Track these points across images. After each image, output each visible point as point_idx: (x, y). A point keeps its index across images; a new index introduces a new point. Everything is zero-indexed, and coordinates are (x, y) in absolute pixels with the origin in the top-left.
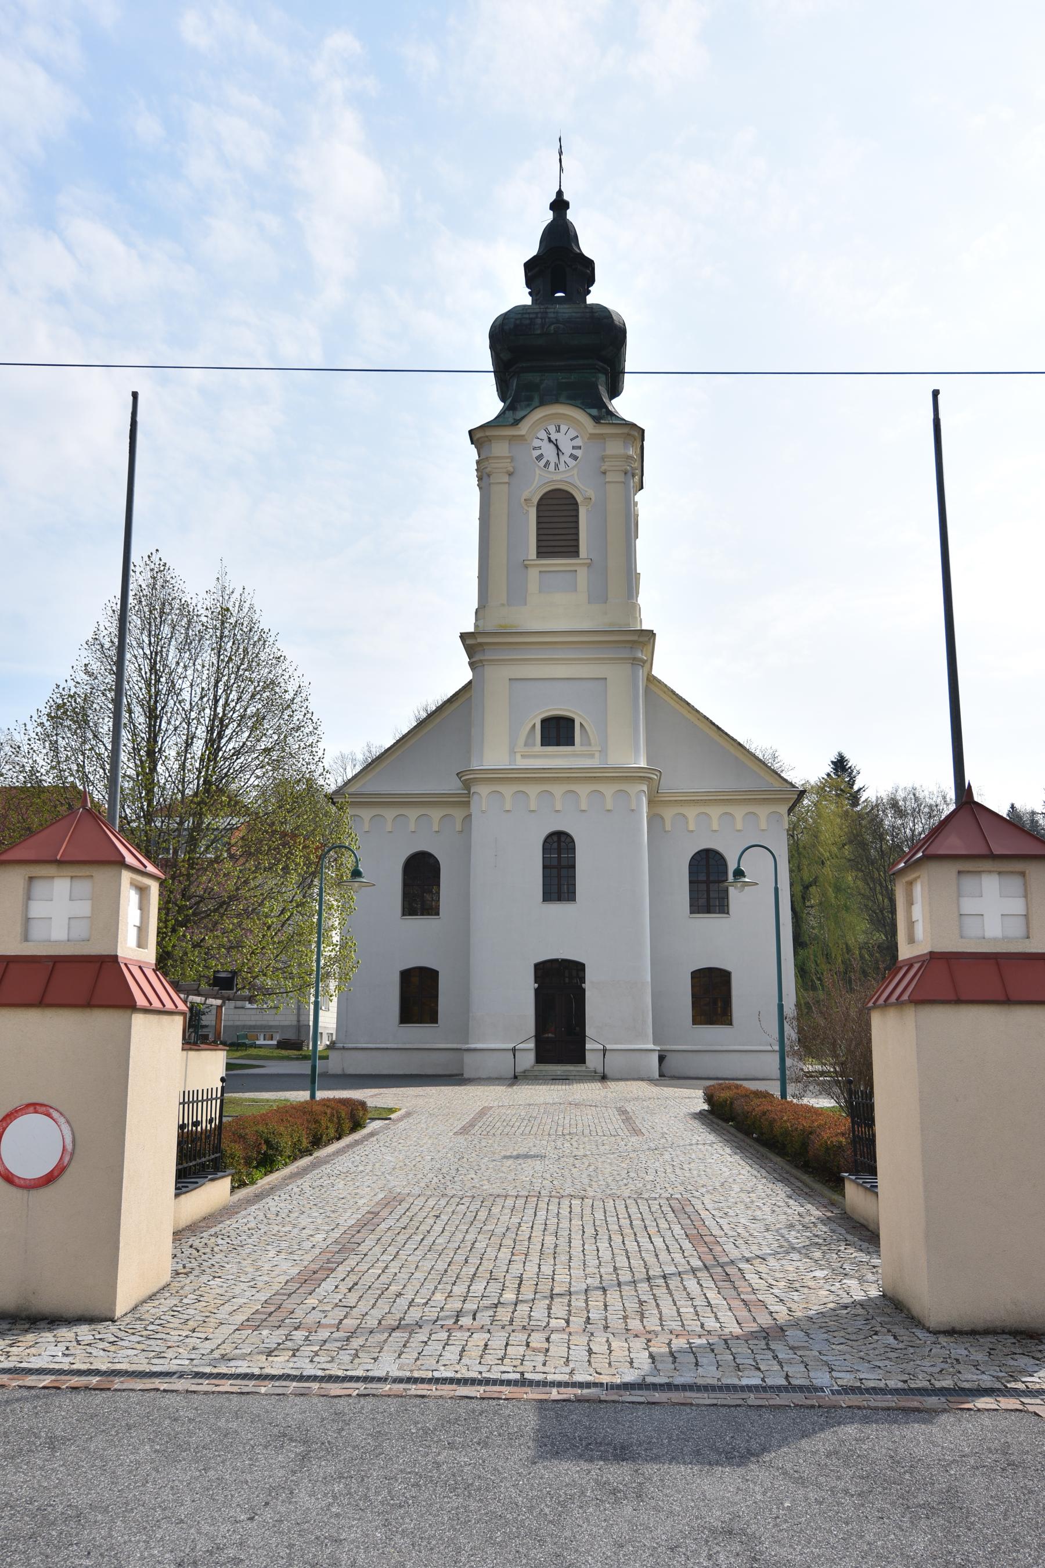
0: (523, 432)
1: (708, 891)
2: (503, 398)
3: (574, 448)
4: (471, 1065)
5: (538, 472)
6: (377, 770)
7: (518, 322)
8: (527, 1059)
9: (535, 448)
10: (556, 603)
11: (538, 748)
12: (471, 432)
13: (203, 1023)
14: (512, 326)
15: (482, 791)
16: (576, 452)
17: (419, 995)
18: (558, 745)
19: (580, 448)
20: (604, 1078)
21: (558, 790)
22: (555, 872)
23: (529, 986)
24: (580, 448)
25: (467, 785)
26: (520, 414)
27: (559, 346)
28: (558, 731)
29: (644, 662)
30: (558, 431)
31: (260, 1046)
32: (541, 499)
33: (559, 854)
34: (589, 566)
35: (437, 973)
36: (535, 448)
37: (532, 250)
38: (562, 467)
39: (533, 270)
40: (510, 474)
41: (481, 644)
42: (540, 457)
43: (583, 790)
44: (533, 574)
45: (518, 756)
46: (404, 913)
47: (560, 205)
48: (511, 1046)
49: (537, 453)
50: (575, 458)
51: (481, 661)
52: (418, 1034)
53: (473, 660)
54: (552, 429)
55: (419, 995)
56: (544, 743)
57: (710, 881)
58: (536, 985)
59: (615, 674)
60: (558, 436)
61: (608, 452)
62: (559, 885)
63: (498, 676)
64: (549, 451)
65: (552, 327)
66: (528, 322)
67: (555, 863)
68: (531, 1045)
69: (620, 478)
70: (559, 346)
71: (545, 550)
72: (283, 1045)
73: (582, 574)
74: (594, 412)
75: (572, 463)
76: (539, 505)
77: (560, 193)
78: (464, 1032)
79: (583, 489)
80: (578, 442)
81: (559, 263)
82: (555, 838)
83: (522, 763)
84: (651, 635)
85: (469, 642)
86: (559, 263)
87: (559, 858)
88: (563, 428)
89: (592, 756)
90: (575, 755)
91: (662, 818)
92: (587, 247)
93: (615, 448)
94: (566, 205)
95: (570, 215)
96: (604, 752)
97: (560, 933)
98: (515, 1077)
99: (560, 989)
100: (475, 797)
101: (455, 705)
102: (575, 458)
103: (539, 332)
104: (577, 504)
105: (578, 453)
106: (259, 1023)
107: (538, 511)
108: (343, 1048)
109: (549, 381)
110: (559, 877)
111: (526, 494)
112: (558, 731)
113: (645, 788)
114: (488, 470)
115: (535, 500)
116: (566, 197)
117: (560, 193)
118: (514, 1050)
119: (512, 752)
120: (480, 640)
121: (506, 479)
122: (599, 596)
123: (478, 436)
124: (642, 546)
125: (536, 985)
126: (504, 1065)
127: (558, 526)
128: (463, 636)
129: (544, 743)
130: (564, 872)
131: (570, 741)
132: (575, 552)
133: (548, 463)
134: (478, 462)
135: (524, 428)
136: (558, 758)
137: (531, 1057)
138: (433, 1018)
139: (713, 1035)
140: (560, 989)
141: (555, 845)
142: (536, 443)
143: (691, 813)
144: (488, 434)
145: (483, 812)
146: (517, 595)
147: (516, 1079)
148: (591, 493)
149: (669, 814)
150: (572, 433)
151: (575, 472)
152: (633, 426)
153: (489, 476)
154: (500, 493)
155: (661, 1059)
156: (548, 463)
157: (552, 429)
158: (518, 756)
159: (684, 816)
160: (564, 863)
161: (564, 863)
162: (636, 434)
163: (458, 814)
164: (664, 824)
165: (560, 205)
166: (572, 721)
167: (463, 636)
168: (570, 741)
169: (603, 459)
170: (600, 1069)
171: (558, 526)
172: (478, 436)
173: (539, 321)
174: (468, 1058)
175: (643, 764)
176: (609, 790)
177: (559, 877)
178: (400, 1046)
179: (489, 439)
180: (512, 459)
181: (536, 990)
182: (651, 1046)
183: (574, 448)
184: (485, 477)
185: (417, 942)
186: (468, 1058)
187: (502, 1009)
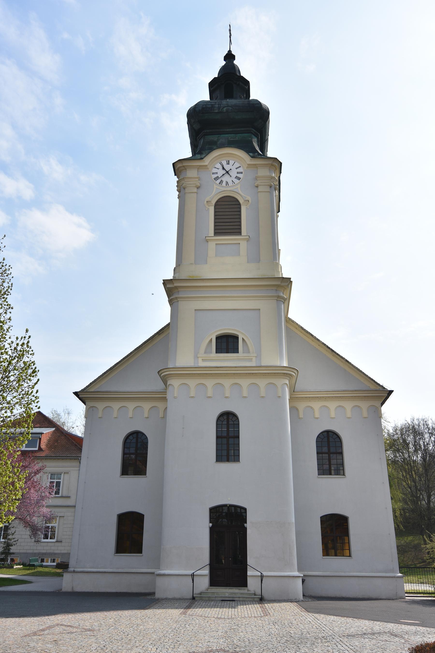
0: (206, 164)
1: (329, 460)
3: (238, 173)
4: (163, 588)
5: (215, 186)
6: (110, 377)
7: (204, 106)
8: (203, 583)
9: (213, 173)
10: (227, 261)
11: (214, 355)
12: (174, 164)
13: (11, 551)
14: (200, 109)
15: (175, 383)
16: (239, 175)
17: (130, 532)
18: (227, 352)
19: (242, 173)
20: (262, 600)
21: (227, 383)
22: (225, 441)
23: (204, 525)
24: (242, 173)
25: (165, 380)
26: (203, 156)
27: (230, 117)
28: (227, 343)
29: (285, 300)
30: (228, 164)
31: (46, 566)
32: (217, 201)
33: (228, 428)
34: (248, 240)
35: (144, 515)
36: (213, 173)
39: (213, 85)
40: (198, 188)
41: (176, 288)
43: (245, 383)
44: (212, 246)
45: (200, 360)
48: (191, 572)
50: (239, 179)
51: (176, 298)
52: (128, 561)
53: (171, 298)
54: (224, 163)
55: (130, 532)
56: (217, 352)
57: (330, 452)
58: (211, 525)
59: (265, 306)
60: (229, 167)
62: (228, 450)
63: (188, 307)
65: (225, 109)
66: (210, 106)
67: (225, 434)
68: (206, 571)
69: (268, 189)
70: (230, 117)
71: (219, 230)
72: (59, 566)
73: (244, 245)
74: (251, 154)
75: (236, 181)
76: (216, 205)
77: (230, 51)
78: (157, 561)
82: (225, 417)
83: (202, 364)
84: (288, 282)
85: (168, 286)
87: (228, 431)
88: (231, 162)
89: (251, 360)
90: (239, 360)
91: (297, 409)
93: (263, 172)
94: (233, 57)
96: (259, 357)
97: (229, 485)
98: (194, 598)
99: (228, 528)
100: (170, 387)
101: (162, 336)
102: (239, 179)
103: (217, 111)
104: (240, 204)
106: (48, 551)
107: (215, 208)
108: (74, 572)
109: (223, 138)
110: (228, 444)
111: (208, 199)
112: (227, 343)
113: (288, 383)
114: (184, 185)
115: (214, 202)
117: (230, 51)
118: (193, 575)
119: (196, 357)
120: (176, 285)
121: (195, 190)
122: (255, 258)
123: (179, 167)
124: (283, 220)
125: (211, 525)
126: (184, 588)
127: (228, 217)
128: (165, 282)
129: (217, 352)
130: (231, 441)
131: (236, 350)
132: (239, 232)
134: (178, 182)
135: (207, 160)
136: (227, 360)
137: (206, 581)
138: (139, 550)
139: (336, 564)
140: (228, 528)
141: (225, 422)
142: (214, 170)
143: (316, 406)
144: (184, 164)
145: (175, 398)
146: (201, 258)
147: (193, 601)
148: (249, 198)
149: (301, 406)
150: (237, 165)
151: (239, 186)
152: (275, 159)
153: (184, 188)
154: (191, 199)
155: (303, 581)
156: (221, 182)
157: (224, 163)
158: (200, 360)
159: (312, 408)
160: (231, 434)
161: (231, 434)
162: (276, 165)
163: (160, 405)
164: (298, 413)
166: (236, 338)
167: (165, 282)
168: (236, 350)
169: (256, 179)
170: (258, 592)
171: (228, 217)
172: (179, 167)
173: (217, 106)
174: (160, 582)
175: (285, 364)
176: (262, 383)
177: (228, 444)
178: (120, 570)
179: (185, 168)
180: (199, 179)
181: (211, 529)
182: (296, 573)
183: (238, 173)
184: (182, 190)
185: (130, 493)
186: (160, 582)
187: (185, 545)
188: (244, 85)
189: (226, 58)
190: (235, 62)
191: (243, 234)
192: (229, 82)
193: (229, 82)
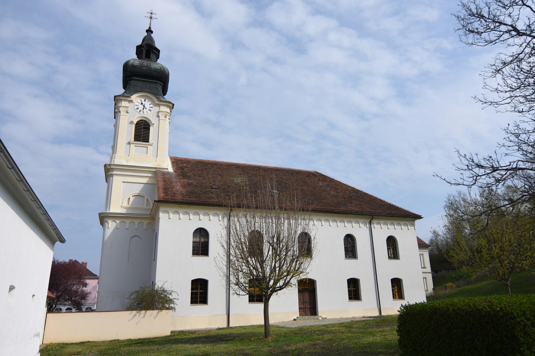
2: (125, 87)
37: (140, 43)
39: (139, 50)
41: (112, 168)
42: (137, 109)
47: (149, 31)
49: (137, 107)
50: (150, 111)
51: (112, 174)
61: (161, 110)
64: (141, 107)
75: (149, 112)
77: (150, 28)
79: (152, 119)
92: (157, 45)
102: (150, 111)
105: (151, 109)
115: (135, 122)
116: (152, 30)
117: (150, 28)
142: (137, 104)
157: (143, 100)
165: (149, 31)
188: (157, 52)
189: (147, 31)
190: (152, 35)
191: (150, 142)
192: (148, 49)
193: (148, 49)
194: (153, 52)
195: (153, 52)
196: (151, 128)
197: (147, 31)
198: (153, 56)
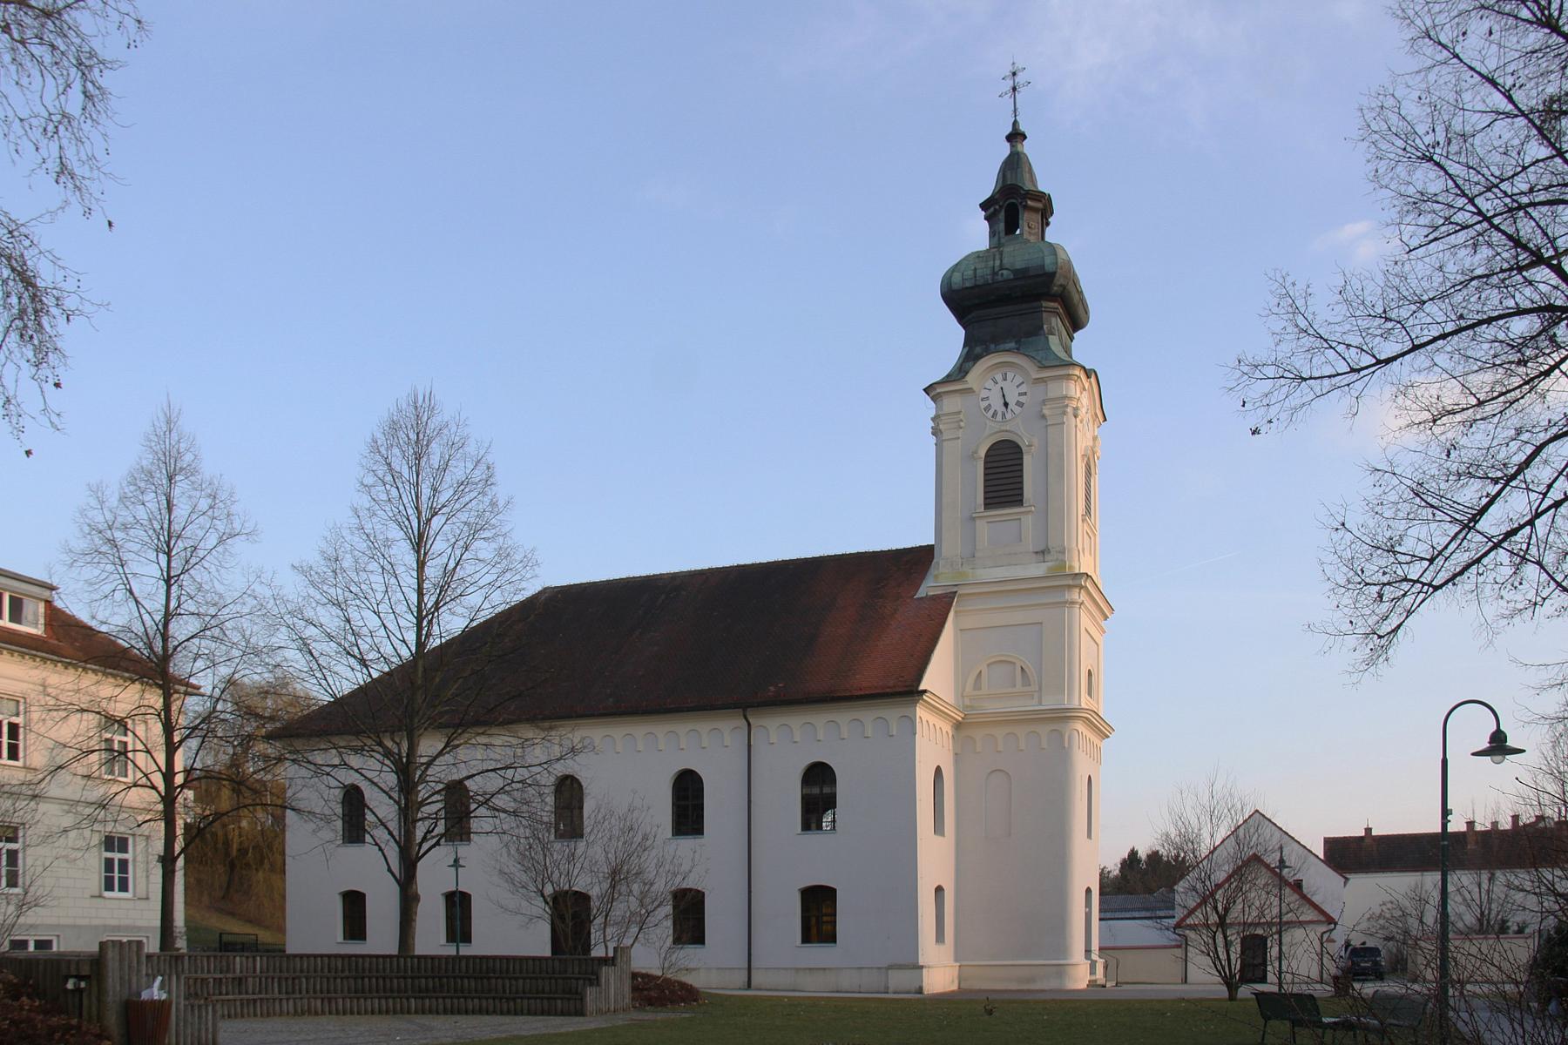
38: (1009, 416)
42: (987, 408)
46: (806, 939)
47: (1016, 136)
49: (985, 404)
75: (1017, 410)
80: (1023, 389)
81: (1015, 203)
86: (1015, 203)
88: (1010, 376)
95: (1027, 147)
105: (1022, 399)
115: (982, 453)
116: (1022, 128)
127: (1004, 477)
133: (995, 414)
142: (984, 394)
150: (1019, 379)
156: (995, 414)
157: (999, 377)
165: (1016, 136)
189: (1010, 138)
194: (1026, 207)
195: (1026, 207)
196: (1027, 460)
197: (1010, 138)
198: (1027, 220)
